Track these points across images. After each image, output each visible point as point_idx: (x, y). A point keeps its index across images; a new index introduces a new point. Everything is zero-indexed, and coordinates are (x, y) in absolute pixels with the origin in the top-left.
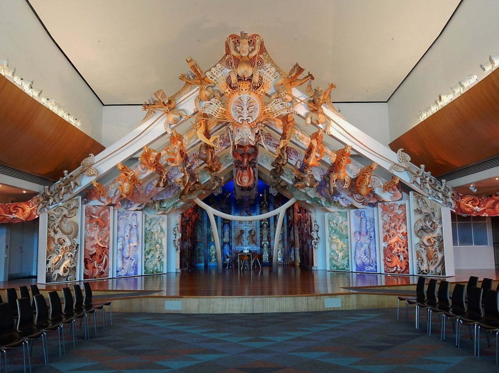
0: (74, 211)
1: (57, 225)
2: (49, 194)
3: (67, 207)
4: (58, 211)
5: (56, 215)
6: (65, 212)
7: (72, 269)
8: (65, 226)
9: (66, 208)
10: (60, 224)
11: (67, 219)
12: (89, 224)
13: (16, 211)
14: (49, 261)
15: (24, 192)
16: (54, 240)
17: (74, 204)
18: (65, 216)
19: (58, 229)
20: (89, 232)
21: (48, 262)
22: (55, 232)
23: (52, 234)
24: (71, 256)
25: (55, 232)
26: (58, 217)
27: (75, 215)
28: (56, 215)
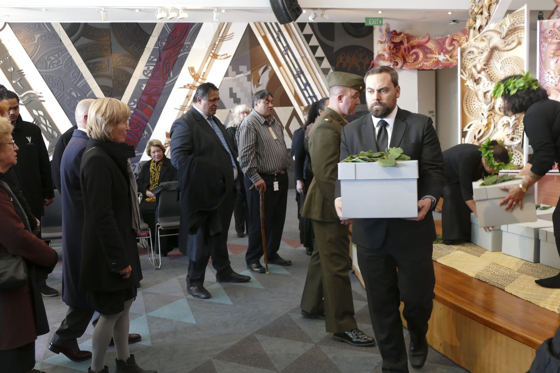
0: (514, 37)
1: (479, 67)
2: (476, 10)
3: (499, 30)
4: (483, 40)
5: (478, 48)
6: (496, 40)
7: (516, 148)
8: (499, 68)
9: (499, 33)
10: (485, 65)
11: (503, 53)
12: (555, 60)
13: (450, 48)
14: (466, 132)
15: (450, 13)
16: (477, 95)
17: (508, 22)
18: (494, 49)
19: (483, 75)
20: (553, 75)
21: (464, 134)
22: (477, 81)
23: (470, 83)
24: (508, 124)
25: (477, 81)
26: (482, 53)
27: (519, 43)
28: (478, 48)
